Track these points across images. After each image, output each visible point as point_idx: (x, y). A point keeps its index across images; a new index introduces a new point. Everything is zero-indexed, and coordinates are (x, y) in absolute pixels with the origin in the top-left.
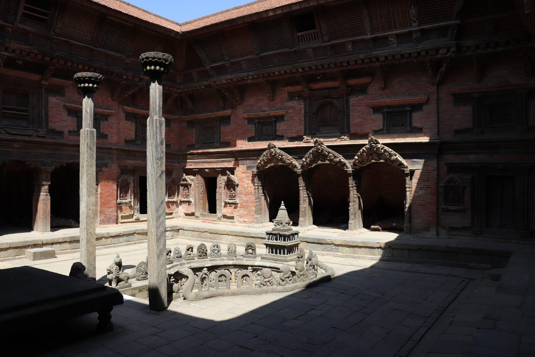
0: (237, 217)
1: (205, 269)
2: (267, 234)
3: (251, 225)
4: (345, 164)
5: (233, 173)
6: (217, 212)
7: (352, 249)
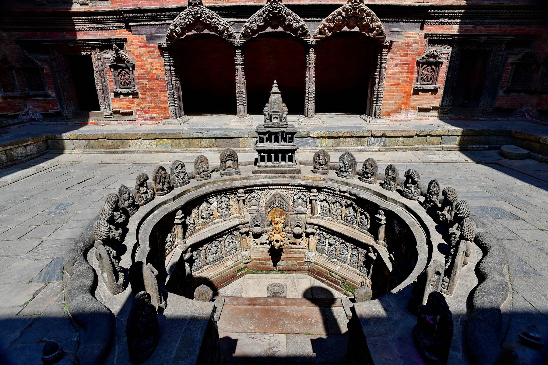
0: (138, 113)
1: (179, 212)
2: (259, 134)
3: (163, 121)
4: (307, 31)
5: (121, 47)
6: (102, 108)
7: (334, 140)
